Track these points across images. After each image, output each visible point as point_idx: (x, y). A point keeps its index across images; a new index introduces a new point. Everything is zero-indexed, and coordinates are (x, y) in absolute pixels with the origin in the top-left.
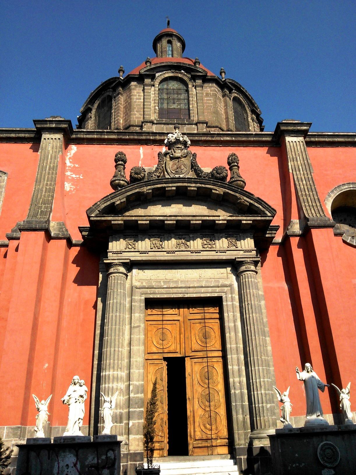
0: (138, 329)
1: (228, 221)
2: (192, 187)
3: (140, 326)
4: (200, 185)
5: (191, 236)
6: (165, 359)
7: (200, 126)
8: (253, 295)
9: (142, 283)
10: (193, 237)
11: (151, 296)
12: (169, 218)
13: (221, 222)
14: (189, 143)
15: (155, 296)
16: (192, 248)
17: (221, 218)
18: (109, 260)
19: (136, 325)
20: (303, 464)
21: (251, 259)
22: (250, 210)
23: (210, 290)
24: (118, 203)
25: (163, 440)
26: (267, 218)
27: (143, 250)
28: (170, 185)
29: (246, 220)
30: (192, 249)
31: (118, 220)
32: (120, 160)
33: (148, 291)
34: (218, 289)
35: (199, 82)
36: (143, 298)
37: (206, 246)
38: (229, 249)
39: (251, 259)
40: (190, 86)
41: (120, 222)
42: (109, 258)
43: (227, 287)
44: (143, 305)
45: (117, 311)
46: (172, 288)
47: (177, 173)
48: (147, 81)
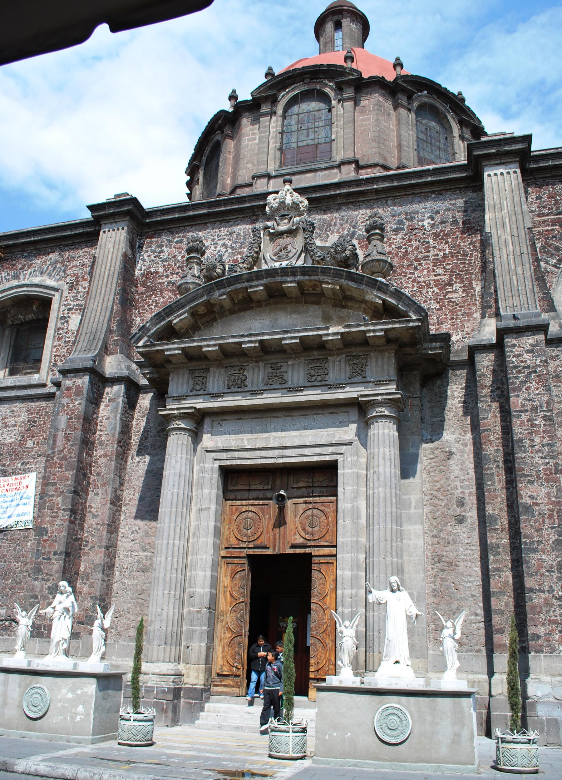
0: (206, 512)
1: (342, 334)
2: (288, 282)
3: (209, 508)
4: (302, 278)
5: (290, 363)
6: (249, 556)
7: (344, 168)
8: (384, 458)
9: (216, 442)
10: (293, 365)
11: (228, 463)
12: (247, 339)
13: (330, 338)
14: (306, 203)
15: (234, 463)
16: (290, 382)
17: (332, 330)
18: (166, 410)
19: (203, 507)
20: (349, 734)
21: (385, 397)
22: (387, 312)
23: (318, 450)
24: (175, 322)
25: (239, 673)
26: (411, 324)
27: (216, 391)
28: (255, 283)
29: (376, 329)
30: (289, 385)
31: (173, 348)
32: (196, 250)
33: (224, 455)
34: (330, 450)
35: (349, 93)
36: (217, 465)
37: (313, 378)
38: (349, 381)
39: (385, 397)
40: (334, 102)
41: (177, 352)
42: (168, 407)
43: (346, 444)
44: (216, 475)
45: (174, 486)
46: (260, 449)
47: (280, 258)
48: (265, 109)
